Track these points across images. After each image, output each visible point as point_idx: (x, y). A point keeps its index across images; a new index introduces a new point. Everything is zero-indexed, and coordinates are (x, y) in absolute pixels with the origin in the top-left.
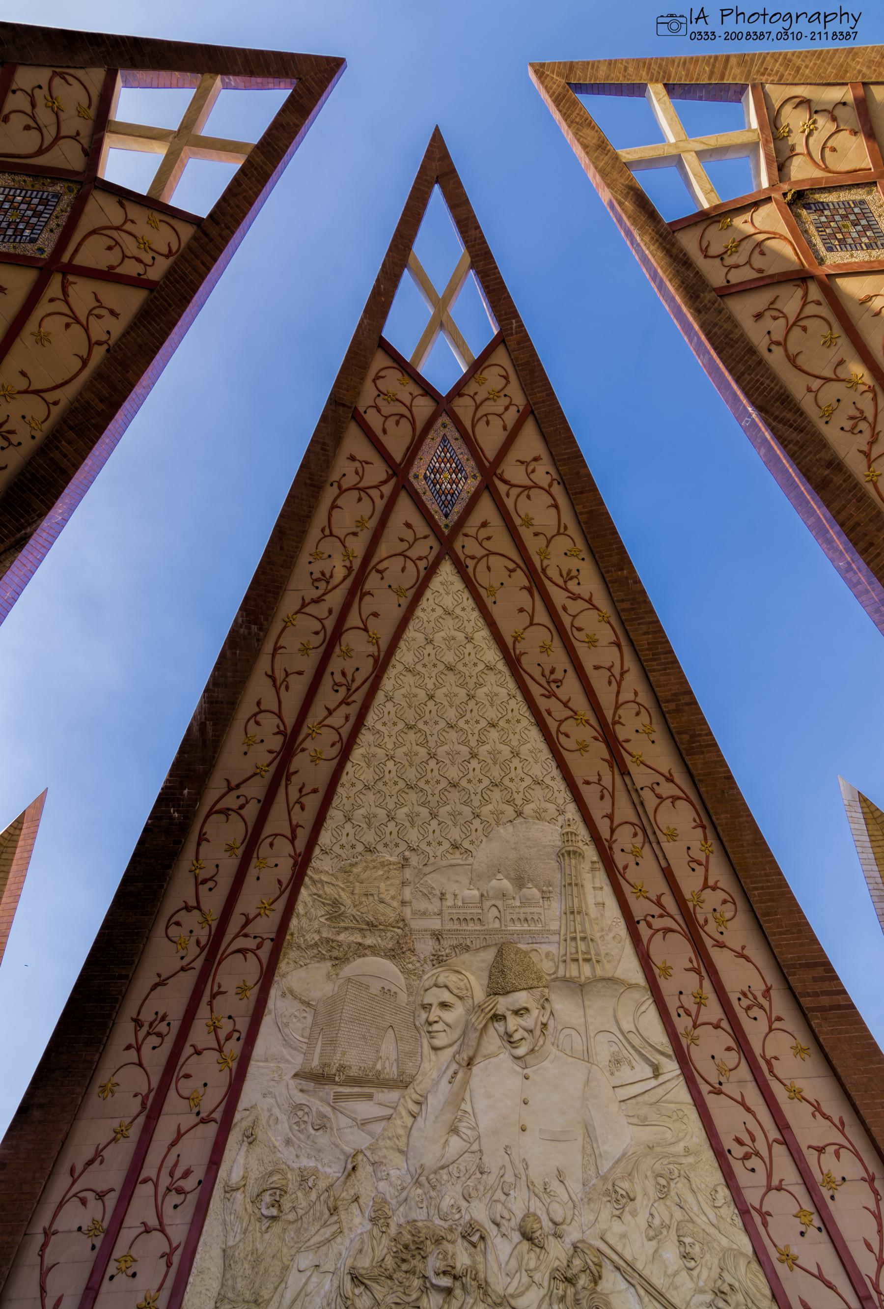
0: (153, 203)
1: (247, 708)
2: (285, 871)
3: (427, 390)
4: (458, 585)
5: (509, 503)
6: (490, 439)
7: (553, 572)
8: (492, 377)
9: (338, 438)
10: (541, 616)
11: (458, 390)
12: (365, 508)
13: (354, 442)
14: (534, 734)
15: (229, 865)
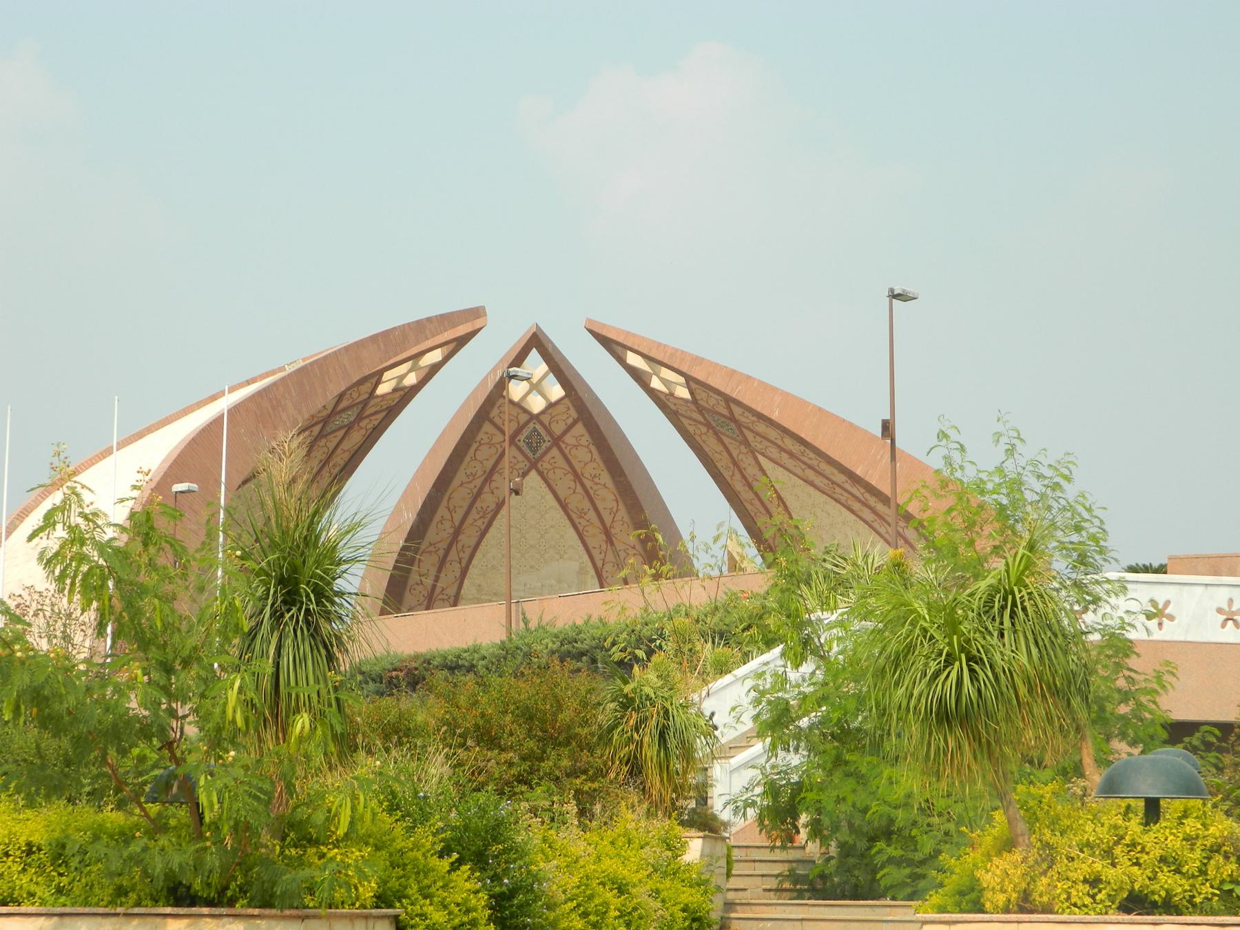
0: (395, 390)
1: (437, 518)
2: (458, 573)
3: (526, 411)
4: (539, 478)
5: (567, 451)
6: (558, 429)
7: (587, 475)
8: (561, 408)
9: (479, 428)
10: (579, 489)
11: (543, 412)
12: (493, 450)
13: (487, 427)
14: (572, 531)
15: (433, 571)
